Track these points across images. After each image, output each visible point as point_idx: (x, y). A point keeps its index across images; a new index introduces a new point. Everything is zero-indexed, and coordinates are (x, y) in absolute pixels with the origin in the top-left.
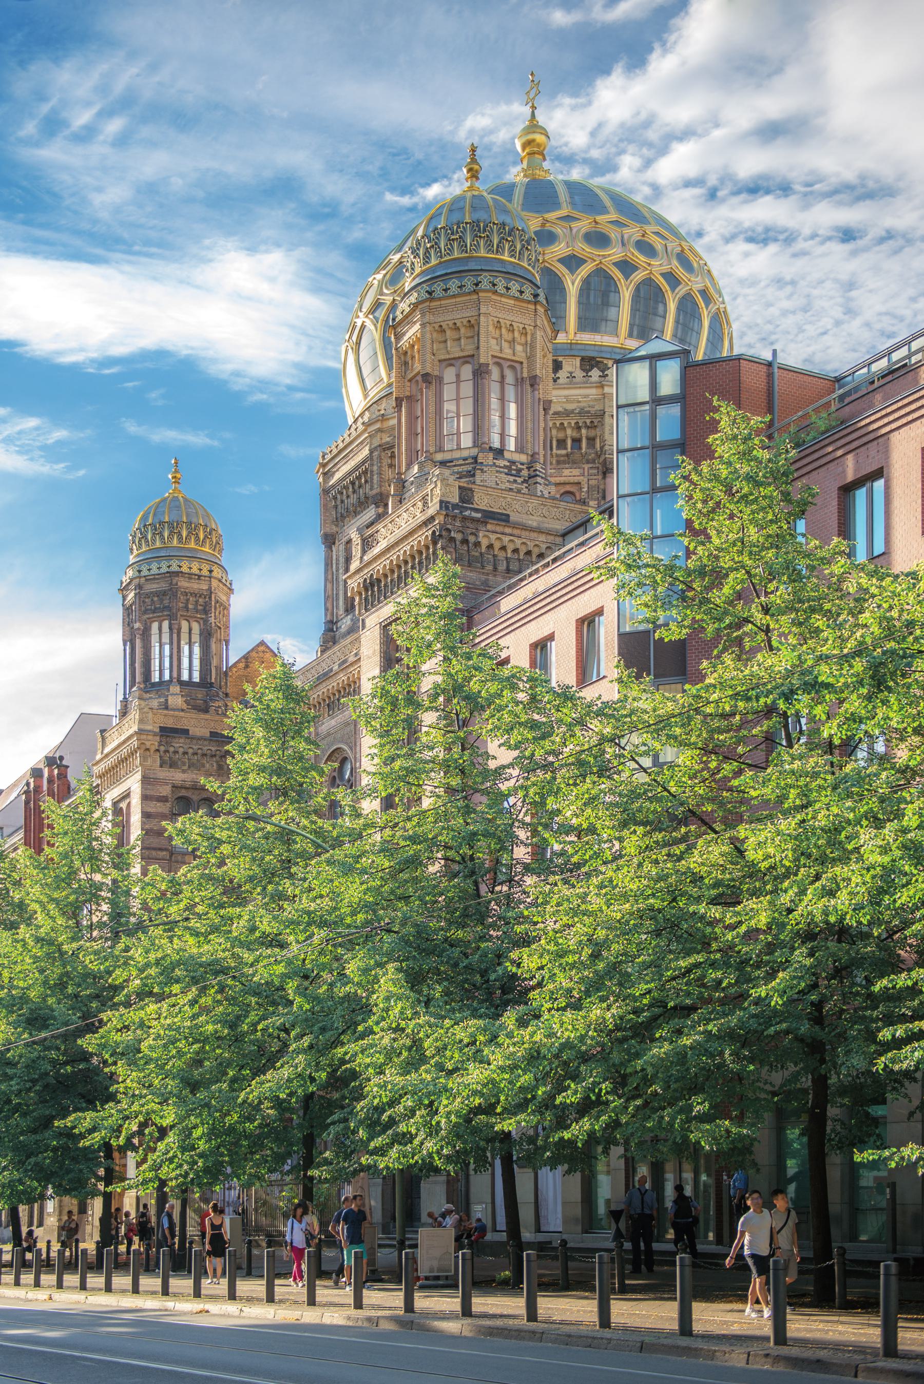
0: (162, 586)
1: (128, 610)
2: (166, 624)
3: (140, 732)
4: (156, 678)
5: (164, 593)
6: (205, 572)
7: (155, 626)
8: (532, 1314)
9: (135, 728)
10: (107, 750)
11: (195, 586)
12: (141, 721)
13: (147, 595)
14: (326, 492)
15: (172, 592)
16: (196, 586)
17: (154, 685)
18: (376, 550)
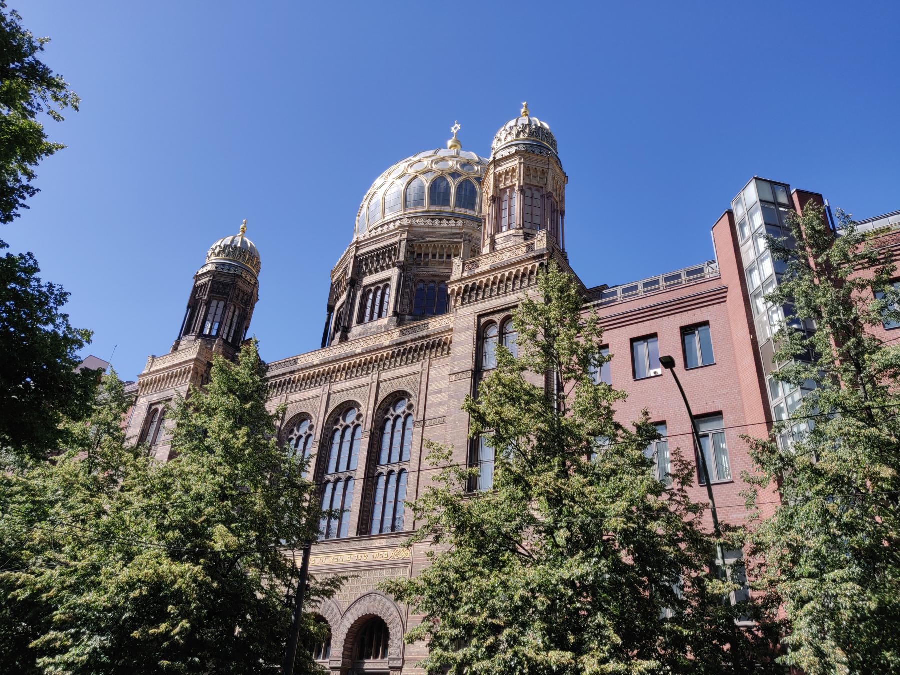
0: (229, 281)
1: (196, 290)
2: (222, 304)
3: (196, 360)
4: (207, 332)
5: (228, 285)
6: (253, 282)
7: (214, 303)
9: (195, 356)
10: (152, 370)
12: (199, 353)
13: (217, 283)
14: (356, 257)
15: (233, 285)
16: (246, 288)
17: (205, 336)
18: (477, 271)
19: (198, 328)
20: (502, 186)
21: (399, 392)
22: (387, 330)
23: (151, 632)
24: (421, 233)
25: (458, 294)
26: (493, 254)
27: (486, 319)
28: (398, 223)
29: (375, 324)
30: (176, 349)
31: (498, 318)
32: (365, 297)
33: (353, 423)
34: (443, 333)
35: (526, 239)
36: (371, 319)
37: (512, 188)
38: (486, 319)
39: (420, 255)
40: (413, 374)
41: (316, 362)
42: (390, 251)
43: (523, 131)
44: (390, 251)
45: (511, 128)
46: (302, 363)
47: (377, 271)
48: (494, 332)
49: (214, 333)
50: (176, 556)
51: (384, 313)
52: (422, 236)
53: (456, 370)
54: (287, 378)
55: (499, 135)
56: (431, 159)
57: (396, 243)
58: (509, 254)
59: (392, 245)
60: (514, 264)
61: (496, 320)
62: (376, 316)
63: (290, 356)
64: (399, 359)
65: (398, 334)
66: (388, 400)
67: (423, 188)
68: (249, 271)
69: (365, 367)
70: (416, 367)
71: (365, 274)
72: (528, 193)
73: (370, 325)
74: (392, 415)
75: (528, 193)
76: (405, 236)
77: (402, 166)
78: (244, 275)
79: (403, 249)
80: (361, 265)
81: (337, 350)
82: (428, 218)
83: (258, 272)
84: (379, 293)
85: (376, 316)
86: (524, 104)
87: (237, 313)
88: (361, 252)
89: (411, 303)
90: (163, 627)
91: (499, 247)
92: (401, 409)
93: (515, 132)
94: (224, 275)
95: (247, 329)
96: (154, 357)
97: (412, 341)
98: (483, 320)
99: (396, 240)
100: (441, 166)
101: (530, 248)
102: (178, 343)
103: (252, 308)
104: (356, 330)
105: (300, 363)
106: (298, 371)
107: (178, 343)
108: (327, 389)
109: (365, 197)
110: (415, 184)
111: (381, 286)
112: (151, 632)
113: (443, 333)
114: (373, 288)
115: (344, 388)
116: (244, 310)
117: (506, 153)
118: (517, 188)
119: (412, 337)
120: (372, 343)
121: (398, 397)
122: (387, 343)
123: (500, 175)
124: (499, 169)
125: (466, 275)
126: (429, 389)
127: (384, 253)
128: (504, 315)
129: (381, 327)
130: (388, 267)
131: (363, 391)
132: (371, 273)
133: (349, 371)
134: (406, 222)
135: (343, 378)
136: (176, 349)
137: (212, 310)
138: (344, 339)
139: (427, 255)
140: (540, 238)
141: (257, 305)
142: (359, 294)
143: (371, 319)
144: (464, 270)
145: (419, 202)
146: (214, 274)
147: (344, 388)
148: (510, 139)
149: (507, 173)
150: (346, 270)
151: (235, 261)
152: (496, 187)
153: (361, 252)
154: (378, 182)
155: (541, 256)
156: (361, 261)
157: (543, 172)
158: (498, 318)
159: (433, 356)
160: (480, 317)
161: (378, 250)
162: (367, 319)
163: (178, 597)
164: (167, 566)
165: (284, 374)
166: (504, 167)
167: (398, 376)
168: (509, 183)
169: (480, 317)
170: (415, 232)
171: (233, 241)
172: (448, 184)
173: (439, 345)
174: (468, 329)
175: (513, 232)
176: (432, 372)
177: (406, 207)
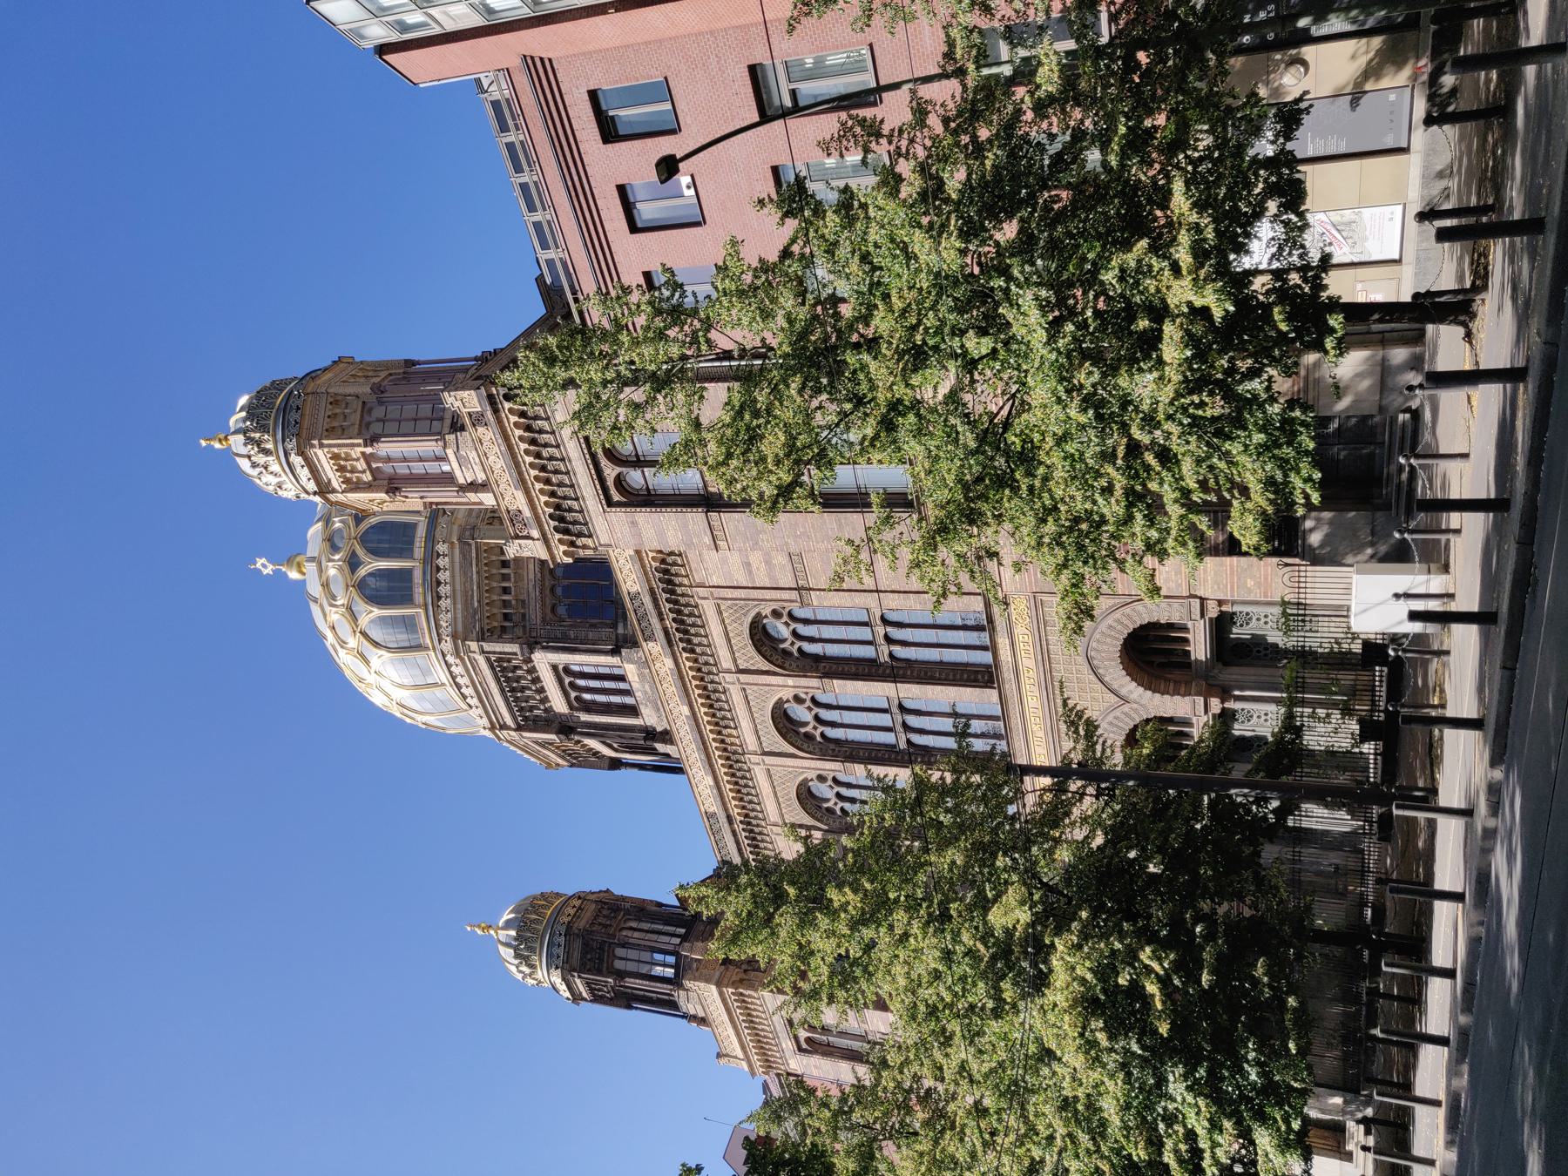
0: (577, 945)
1: (598, 999)
2: (620, 952)
3: (719, 984)
4: (670, 972)
6: (577, 903)
7: (619, 965)
8: (1449, 973)
9: (713, 988)
10: (741, 1055)
11: (588, 915)
12: (708, 981)
14: (519, 728)
15: (586, 937)
17: (677, 974)
18: (527, 513)
19: (664, 988)
20: (367, 477)
21: (752, 636)
22: (646, 664)
23: (1159, 1006)
24: (465, 617)
25: (572, 544)
26: (494, 487)
27: (613, 491)
28: (450, 659)
29: (636, 686)
30: (703, 1021)
31: (610, 471)
32: (589, 707)
33: (810, 709)
34: (643, 566)
35: (463, 428)
36: (627, 693)
37: (368, 458)
38: (613, 491)
39: (506, 617)
40: (720, 613)
41: (710, 781)
42: (504, 670)
43: (258, 443)
44: (504, 670)
45: (254, 465)
46: (712, 805)
47: (542, 690)
48: (635, 477)
49: (671, 959)
50: (1039, 982)
51: (617, 672)
52: (470, 615)
53: (708, 540)
54: (739, 827)
55: (271, 488)
56: (327, 608)
57: (488, 660)
58: (491, 458)
59: (492, 667)
60: (510, 447)
61: (614, 474)
62: (622, 686)
63: (701, 826)
64: (696, 640)
65: (651, 644)
66: (768, 654)
67: (382, 619)
68: (559, 911)
69: (712, 697)
70: (708, 609)
71: (548, 710)
72: (376, 428)
73: (638, 694)
74: (793, 644)
75: (376, 428)
76: (474, 645)
77: (345, 659)
78: (566, 920)
79: (498, 647)
80: (533, 719)
81: (686, 747)
82: (436, 607)
83: (558, 895)
84: (581, 682)
85: (622, 686)
86: (203, 443)
87: (634, 924)
88: (509, 721)
89: (593, 626)
90: (1152, 988)
91: (481, 477)
92: (782, 630)
93: (261, 459)
94: (568, 953)
95: (660, 905)
96: (719, 1055)
97: (662, 620)
98: (616, 497)
99: (481, 660)
100: (338, 588)
101: (477, 420)
102: (693, 1018)
103: (623, 899)
104: (649, 718)
105: (713, 809)
106: (726, 810)
107: (693, 1018)
108: (755, 759)
109: (408, 721)
110: (376, 634)
111: (567, 680)
112: (1159, 1006)
113: (643, 566)
114: (573, 694)
115: (752, 728)
116: (628, 912)
117: (304, 473)
118: (369, 450)
119: (655, 621)
120: (671, 688)
121: (760, 636)
122: (669, 663)
123: (347, 481)
124: (335, 484)
125: (535, 533)
126: (745, 584)
127: (508, 680)
128: (604, 462)
129: (641, 676)
130: (532, 670)
131: (755, 696)
132: (545, 700)
133: (721, 722)
134: (447, 645)
135: (734, 732)
136: (703, 1021)
137: (631, 967)
138: (666, 736)
139: (506, 604)
140: (458, 404)
141: (618, 891)
142: (585, 717)
143: (627, 693)
144: (528, 537)
145: (408, 624)
146: (568, 969)
147: (752, 728)
148: (275, 467)
149: (341, 469)
150: (543, 744)
151: (543, 937)
152: (369, 487)
153: (509, 721)
154: (378, 699)
155: (491, 399)
156: (526, 719)
157: (335, 403)
158: (610, 471)
159: (686, 581)
160: (610, 503)
161: (502, 691)
162: (628, 700)
163: (1105, 972)
164: (1060, 992)
165: (734, 833)
166: (331, 475)
167: (726, 640)
168: (361, 465)
169: (610, 503)
170: (465, 627)
171: (507, 945)
172: (370, 574)
173: (666, 572)
174: (634, 523)
175: (450, 452)
176: (715, 581)
177: (419, 647)
